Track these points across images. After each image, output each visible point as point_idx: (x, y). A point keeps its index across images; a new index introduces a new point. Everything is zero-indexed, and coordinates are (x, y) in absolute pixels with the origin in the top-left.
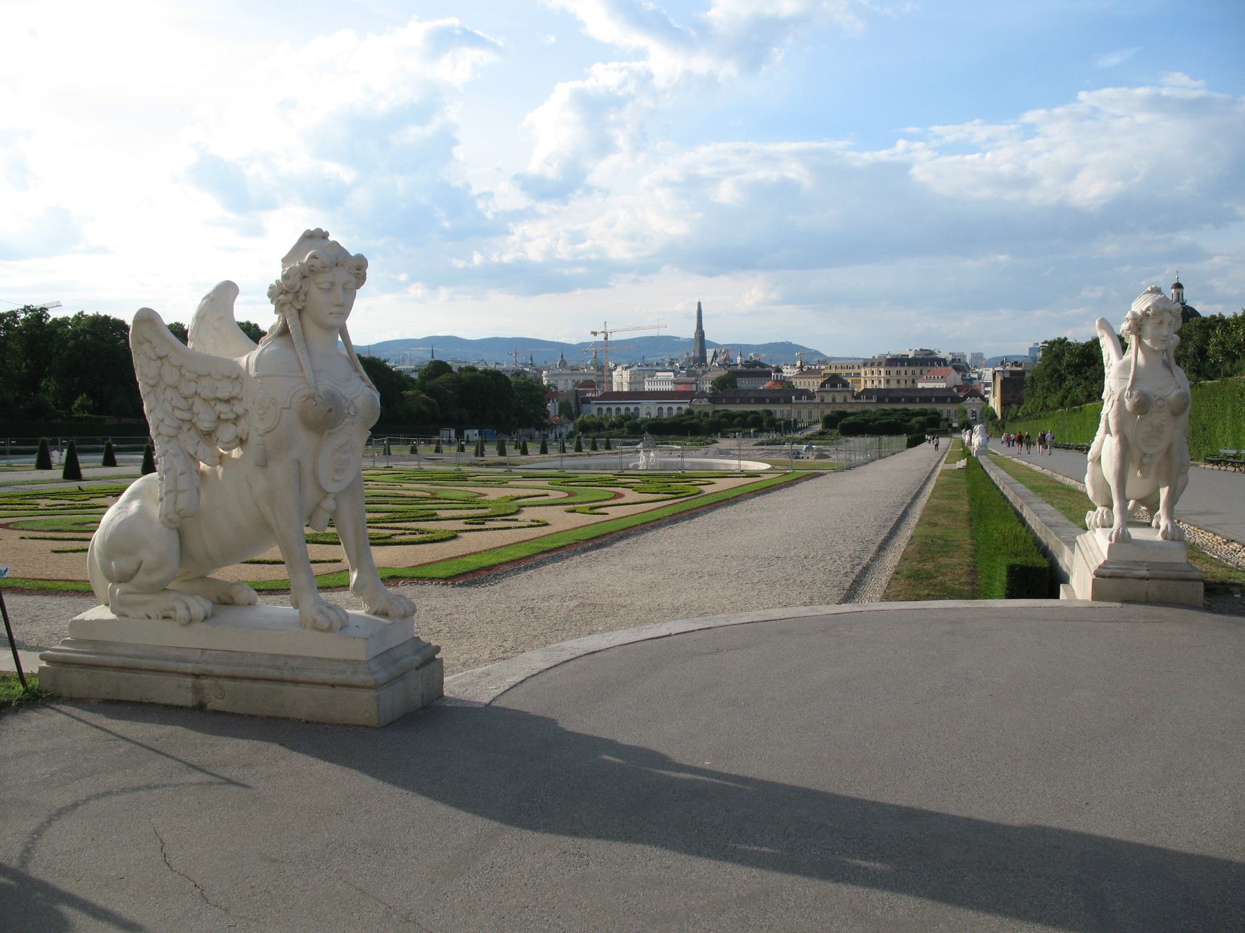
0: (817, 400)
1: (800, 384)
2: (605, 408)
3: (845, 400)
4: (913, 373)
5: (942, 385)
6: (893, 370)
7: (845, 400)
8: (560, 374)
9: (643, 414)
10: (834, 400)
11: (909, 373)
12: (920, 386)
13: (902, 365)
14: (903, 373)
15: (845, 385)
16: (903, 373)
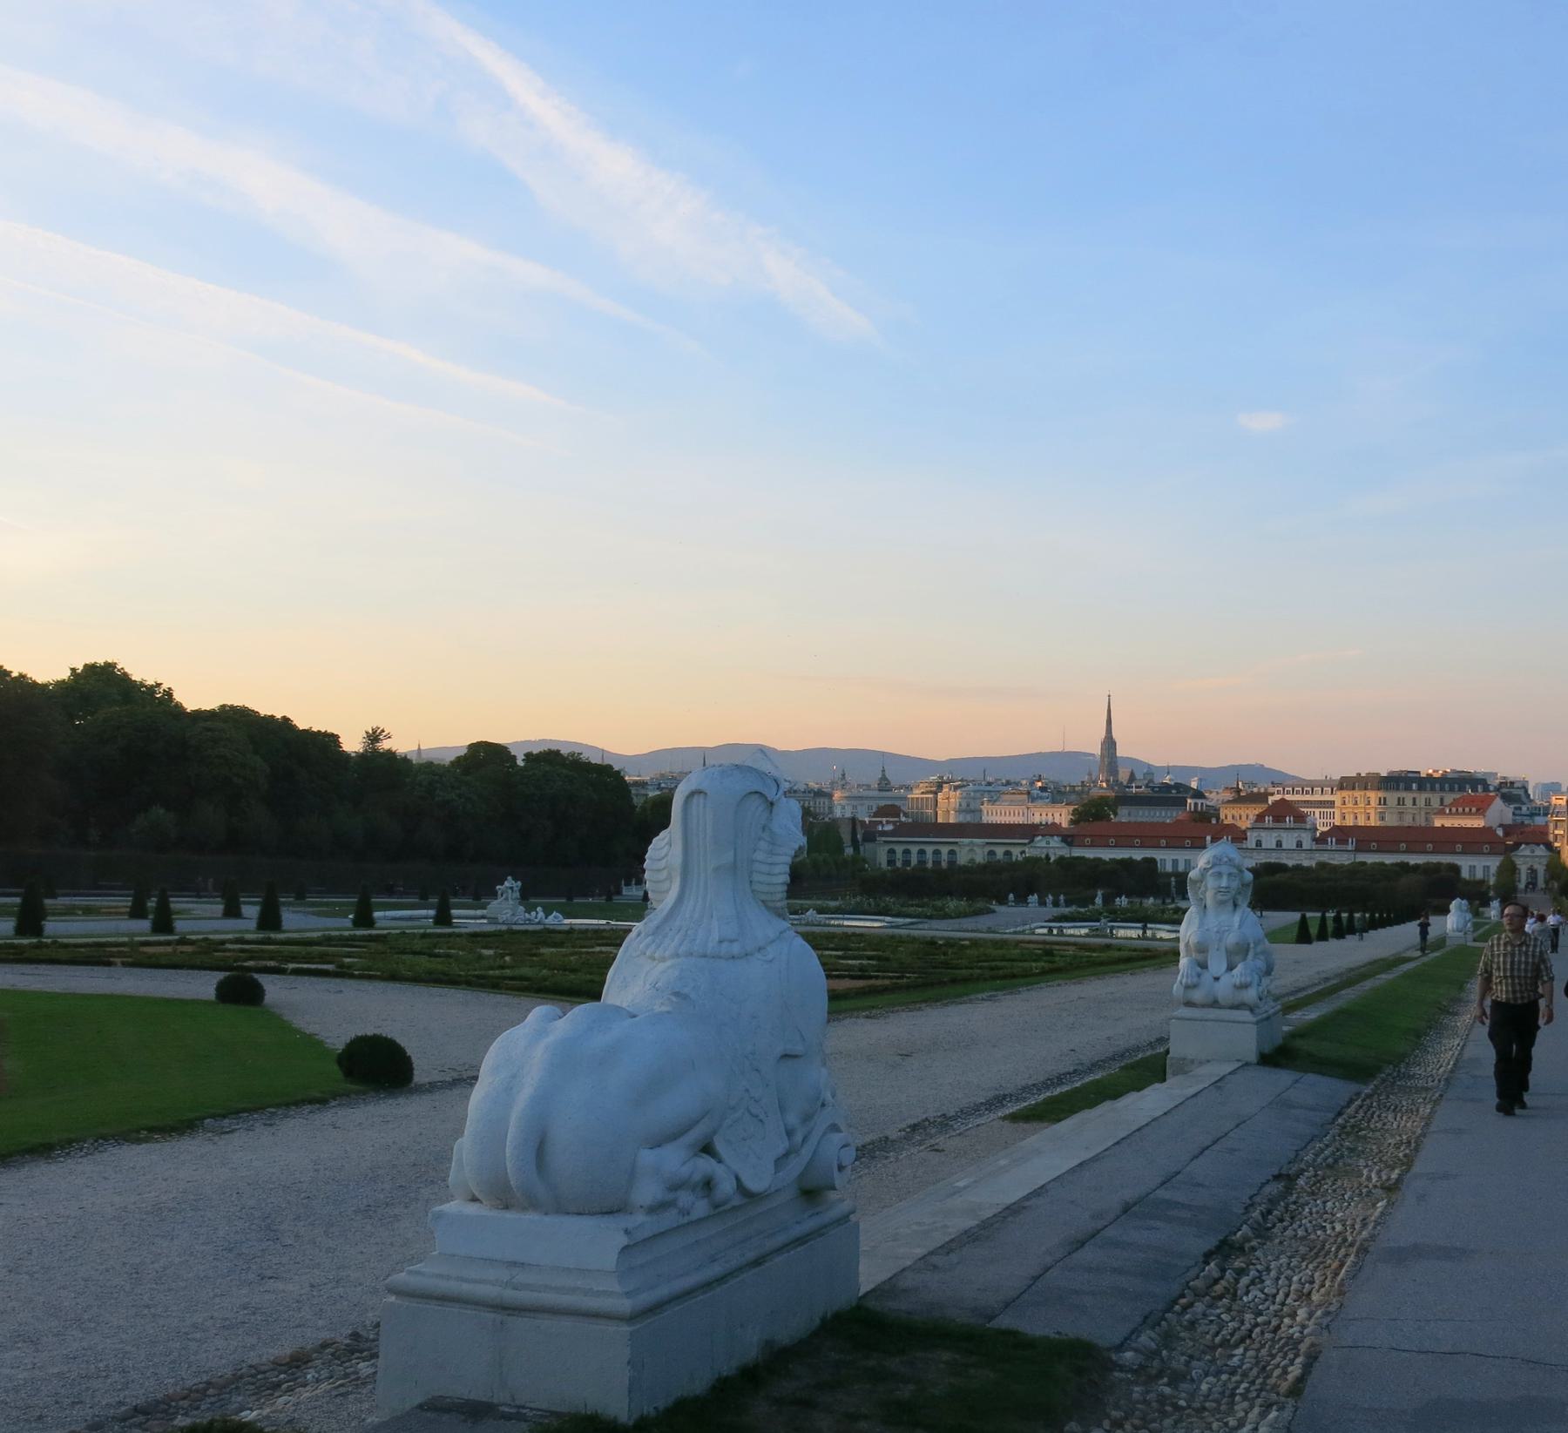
0: (1251, 843)
1: (1228, 815)
2: (899, 849)
3: (1299, 844)
4: (1428, 802)
5: (1477, 823)
6: (1392, 797)
7: (1299, 844)
8: (861, 798)
9: (963, 859)
10: (1279, 844)
11: (1421, 802)
12: (1438, 823)
13: (1408, 789)
14: (1409, 802)
15: (1301, 818)
16: (1409, 802)
